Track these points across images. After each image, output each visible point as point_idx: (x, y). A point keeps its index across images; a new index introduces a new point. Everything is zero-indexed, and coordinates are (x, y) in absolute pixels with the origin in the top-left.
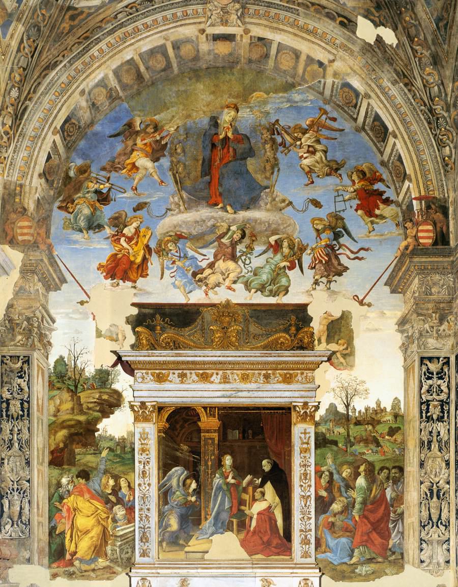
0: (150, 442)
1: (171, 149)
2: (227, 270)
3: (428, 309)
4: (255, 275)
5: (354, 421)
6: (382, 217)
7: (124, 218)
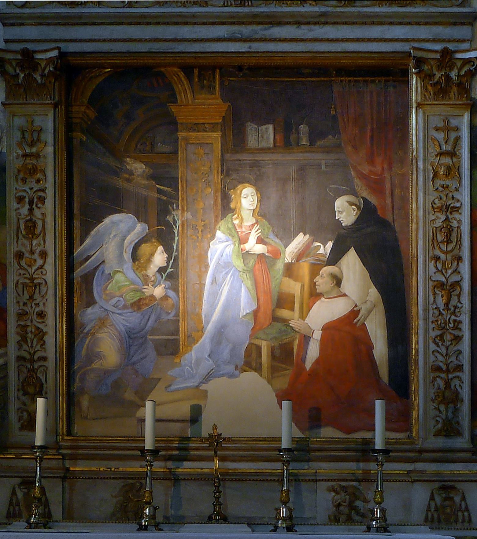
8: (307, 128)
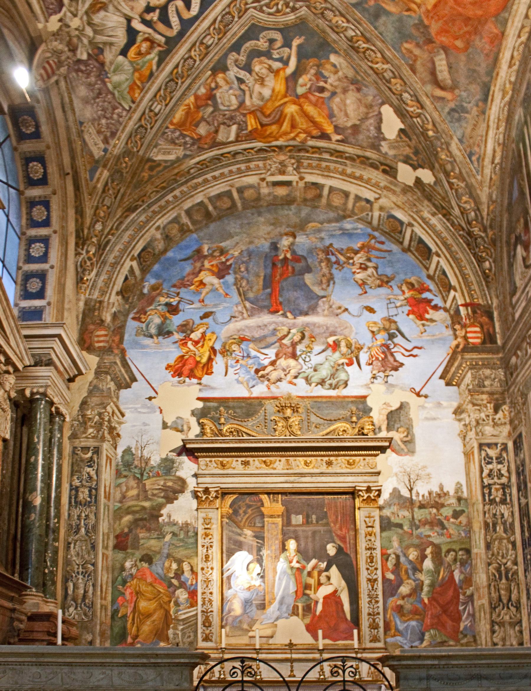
0: (214, 526)
1: (235, 268)
2: (288, 367)
3: (482, 400)
4: (315, 370)
5: (418, 504)
6: (432, 321)
7: (191, 324)
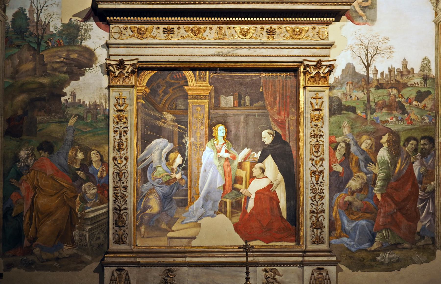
0: (128, 108)
8: (249, 97)
